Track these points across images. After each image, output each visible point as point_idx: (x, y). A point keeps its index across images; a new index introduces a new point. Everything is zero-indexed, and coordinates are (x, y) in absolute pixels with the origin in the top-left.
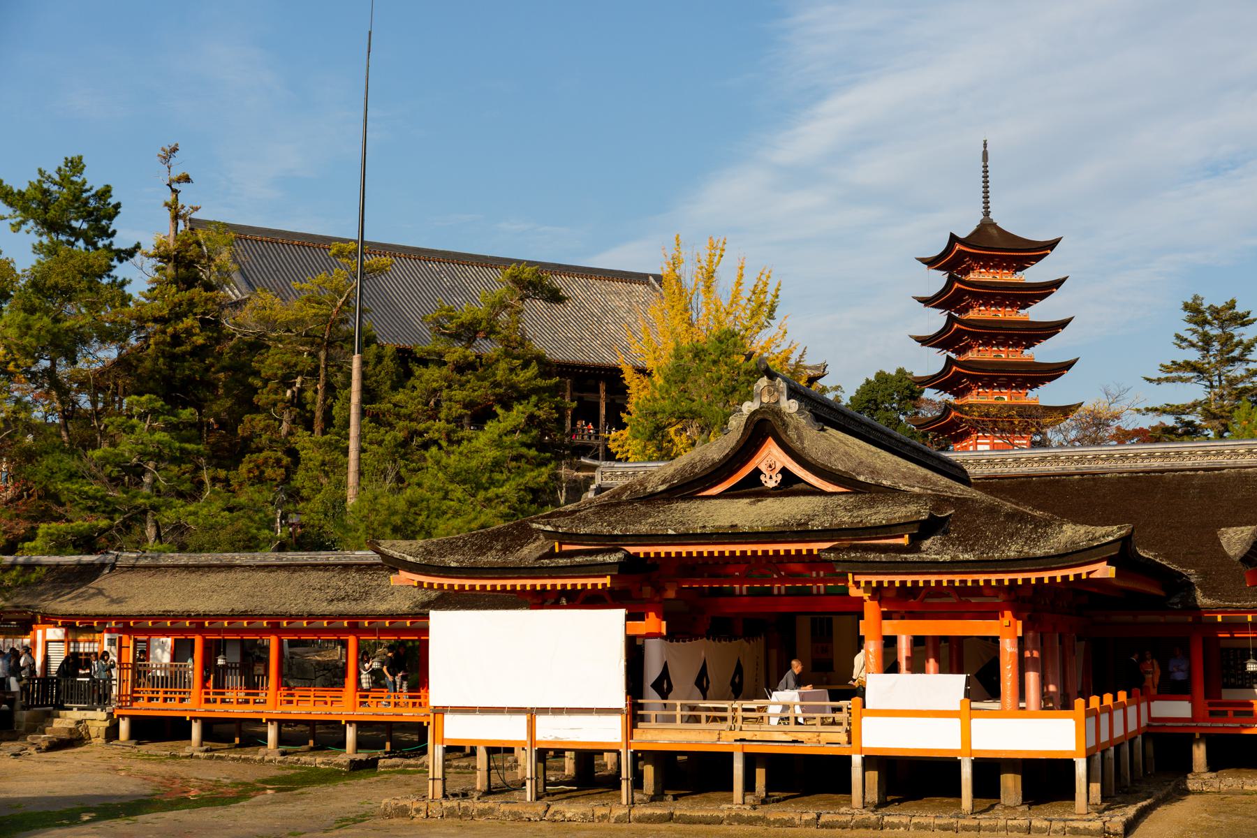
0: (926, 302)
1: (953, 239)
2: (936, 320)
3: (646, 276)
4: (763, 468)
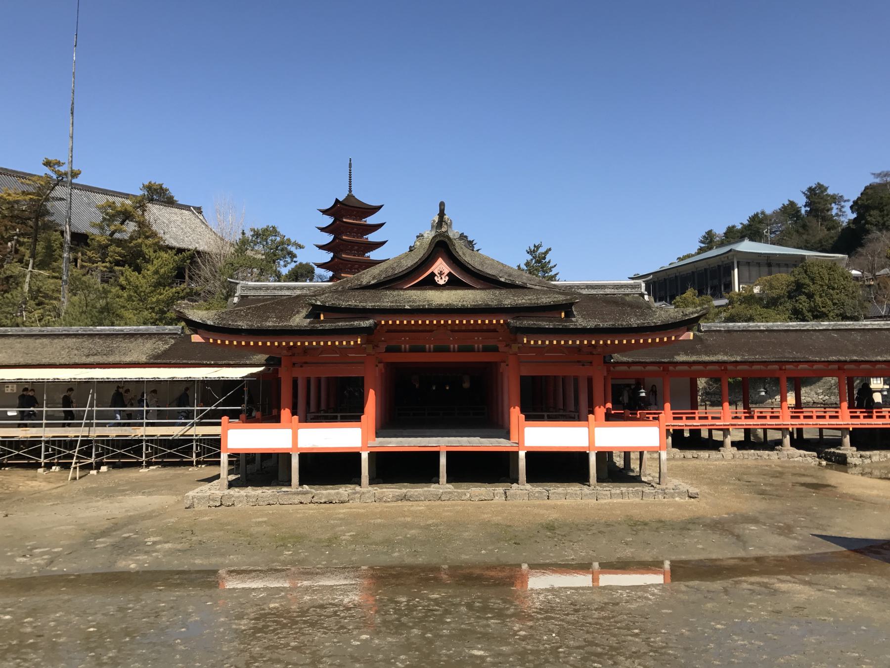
0: (322, 230)
1: (337, 201)
2: (328, 238)
3: (189, 207)
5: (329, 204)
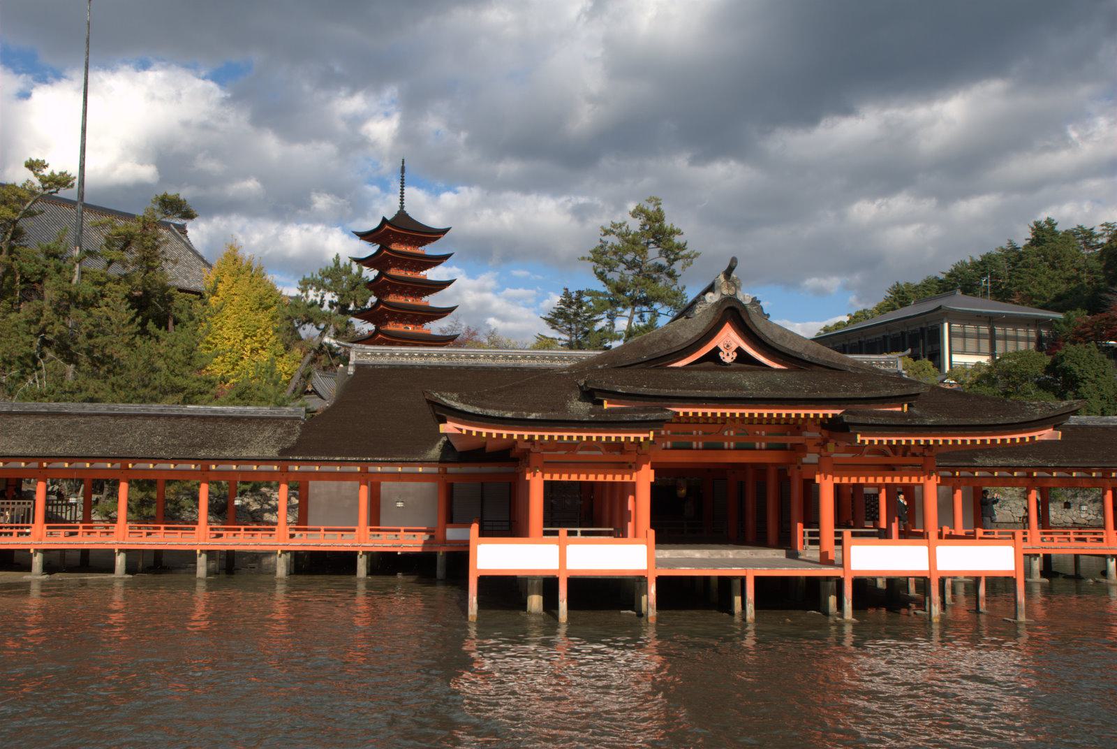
1: (384, 220)
4: (722, 347)
5: (372, 224)
